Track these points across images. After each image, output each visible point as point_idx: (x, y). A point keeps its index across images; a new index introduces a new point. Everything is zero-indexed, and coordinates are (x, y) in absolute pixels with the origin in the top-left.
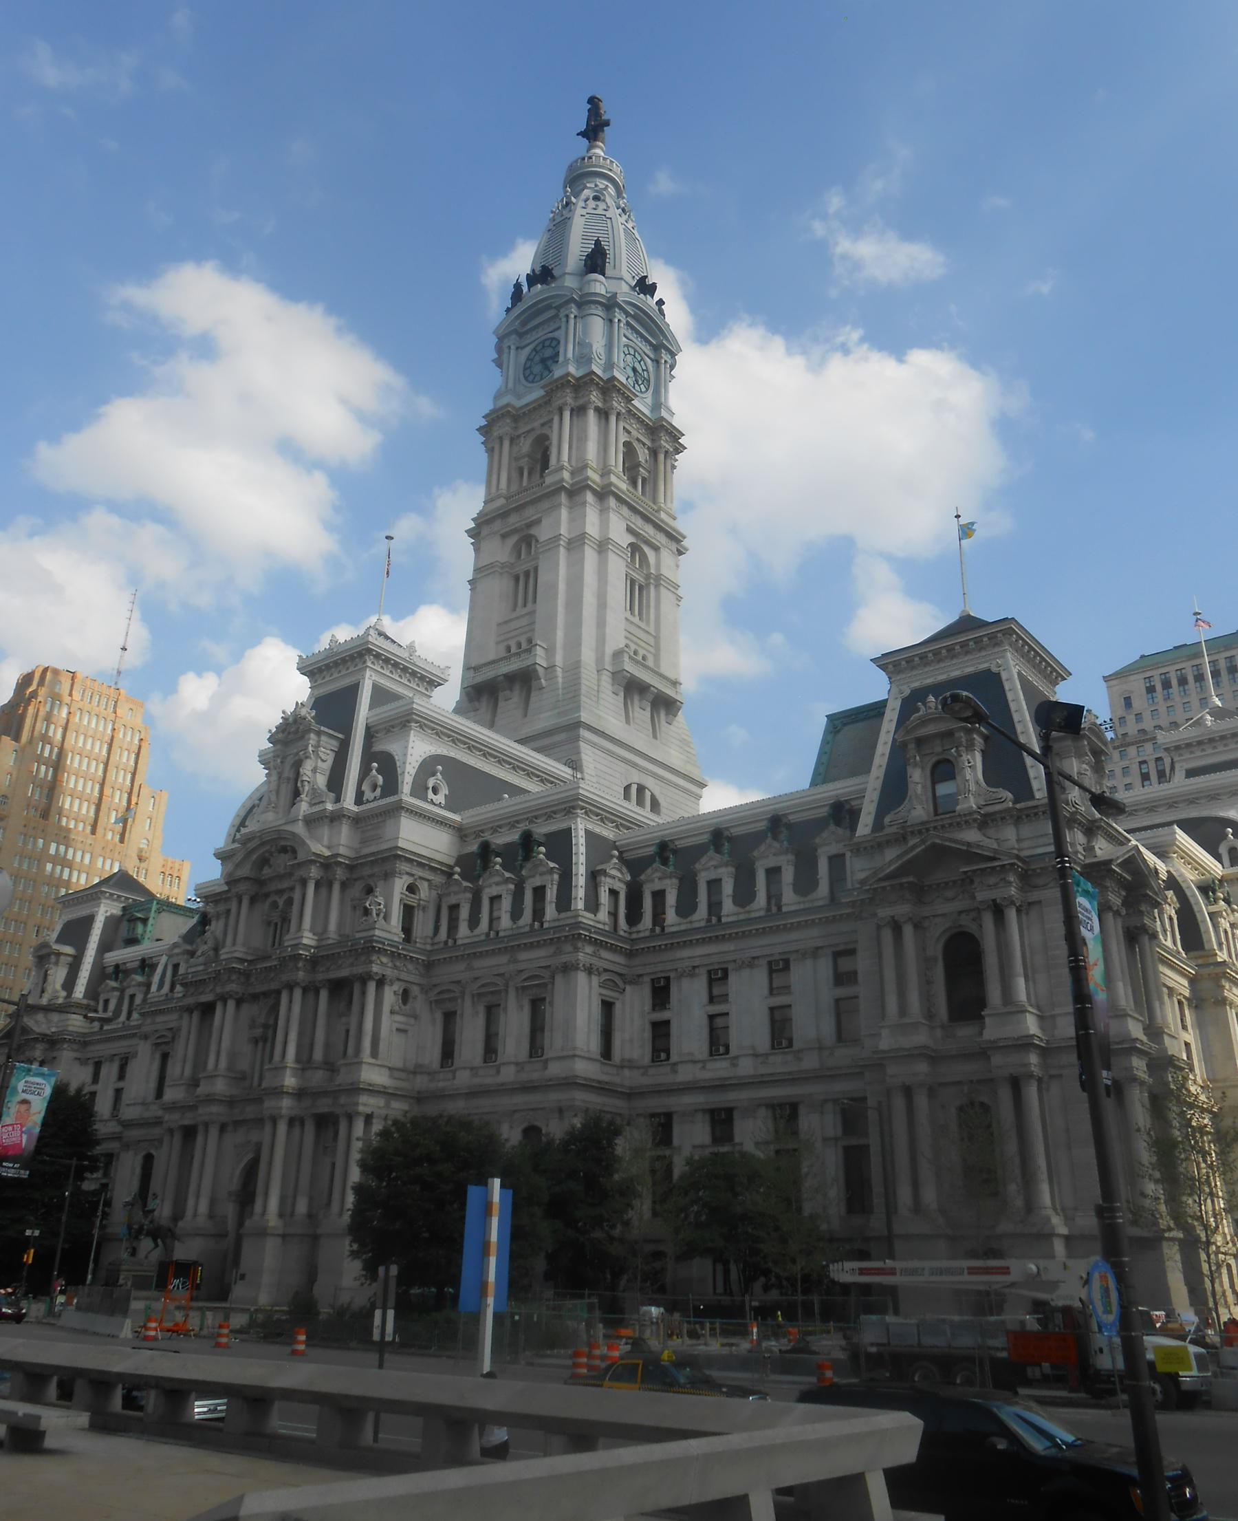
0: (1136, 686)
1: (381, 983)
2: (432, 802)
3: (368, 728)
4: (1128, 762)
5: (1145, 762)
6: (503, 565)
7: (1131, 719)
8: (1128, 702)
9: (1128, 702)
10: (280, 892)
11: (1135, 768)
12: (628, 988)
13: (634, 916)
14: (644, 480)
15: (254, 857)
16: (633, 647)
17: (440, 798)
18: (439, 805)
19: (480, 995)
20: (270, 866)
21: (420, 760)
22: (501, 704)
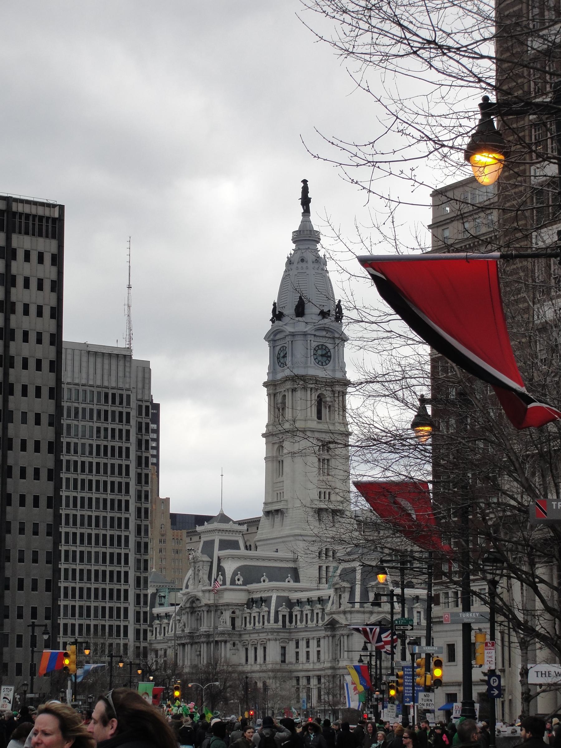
1: (225, 642)
2: (238, 585)
3: (219, 557)
6: (273, 457)
10: (200, 611)
12: (290, 642)
13: (291, 622)
14: (330, 407)
15: (190, 600)
16: (323, 491)
17: (240, 582)
18: (240, 585)
19: (252, 645)
21: (233, 571)
22: (275, 519)
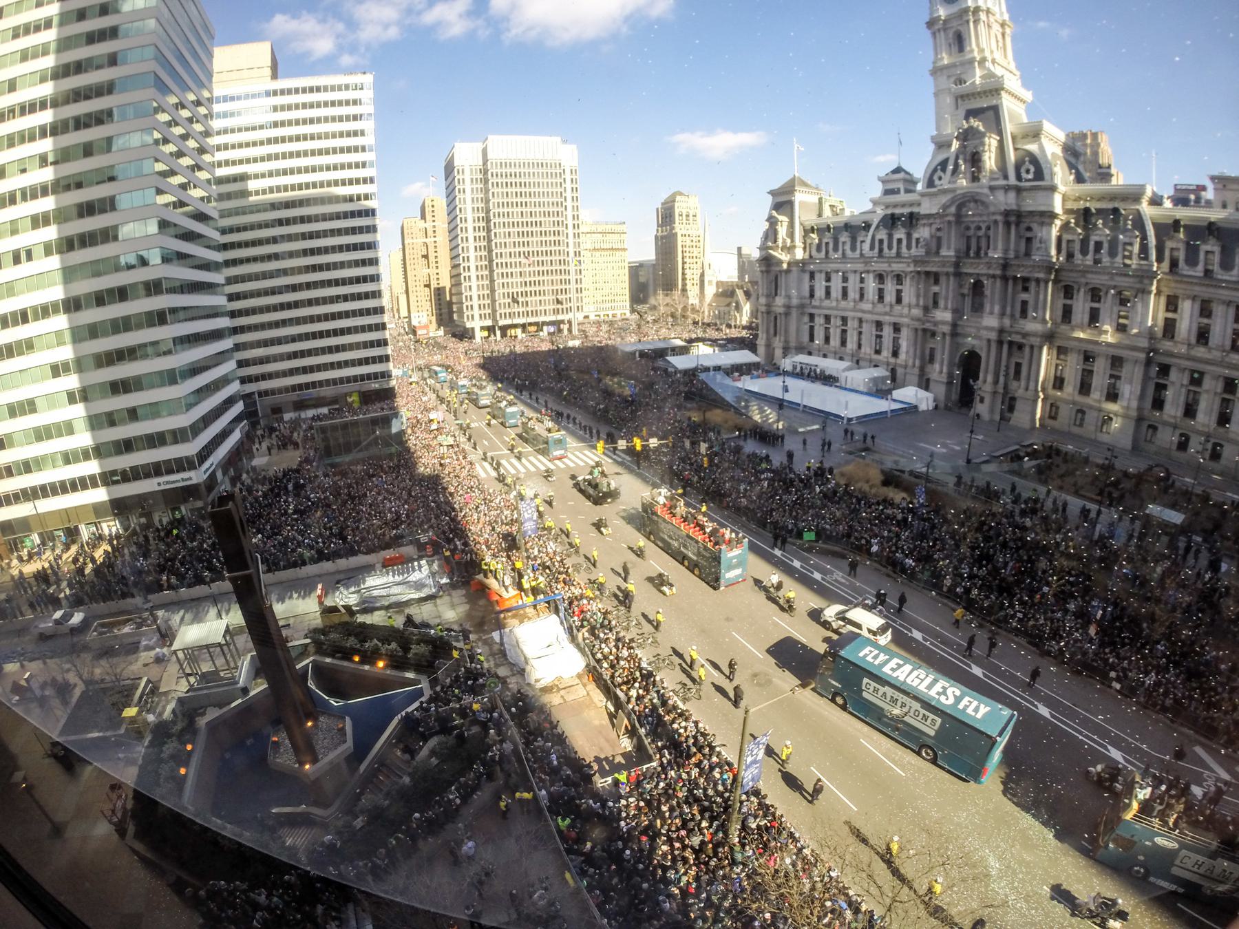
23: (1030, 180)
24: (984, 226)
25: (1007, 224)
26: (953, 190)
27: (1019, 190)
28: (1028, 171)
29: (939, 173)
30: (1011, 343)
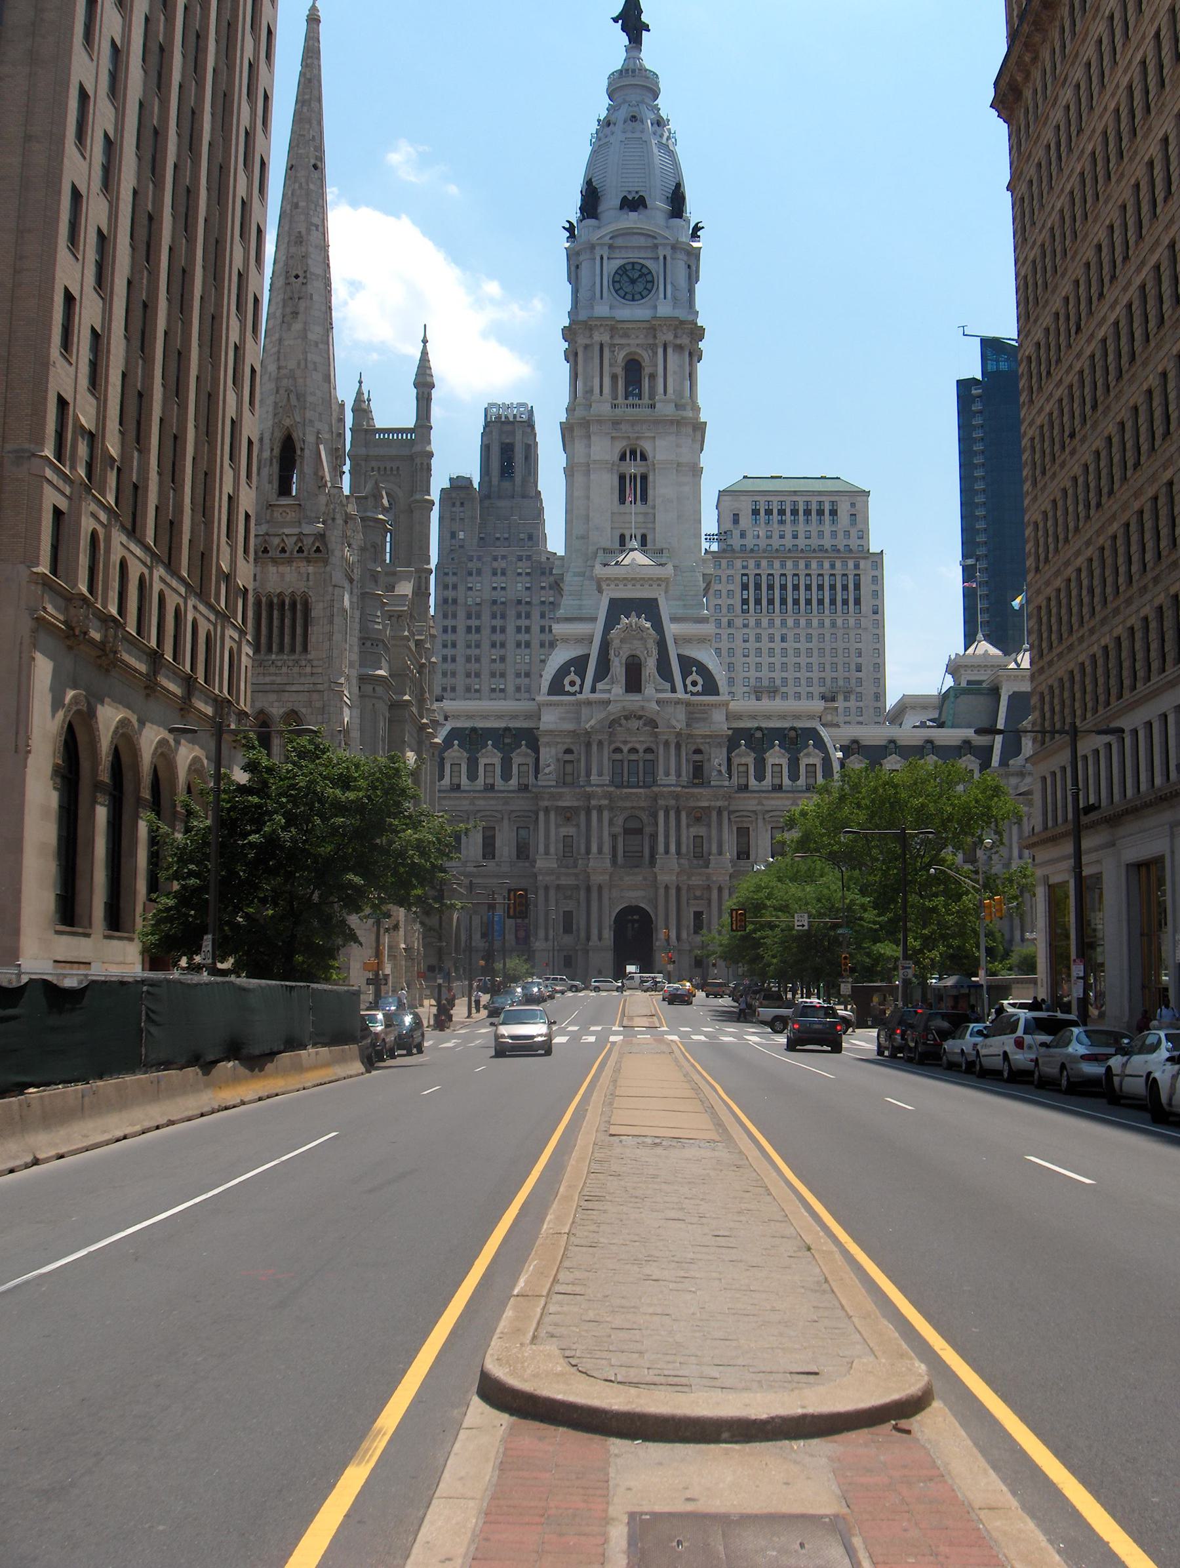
0: (746, 508)
4: (733, 572)
5: (746, 575)
7: (736, 533)
8: (736, 519)
9: (736, 519)
11: (738, 579)
20: (621, 725)
23: (698, 694)
24: (641, 748)
25: (678, 746)
26: (609, 702)
27: (688, 704)
28: (694, 684)
29: (573, 676)
30: (689, 888)
